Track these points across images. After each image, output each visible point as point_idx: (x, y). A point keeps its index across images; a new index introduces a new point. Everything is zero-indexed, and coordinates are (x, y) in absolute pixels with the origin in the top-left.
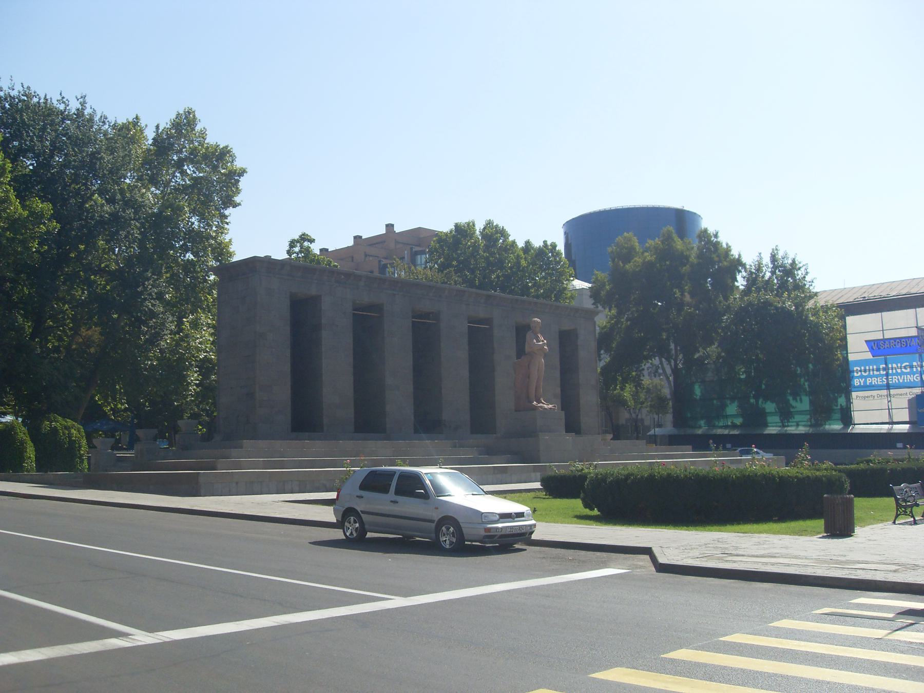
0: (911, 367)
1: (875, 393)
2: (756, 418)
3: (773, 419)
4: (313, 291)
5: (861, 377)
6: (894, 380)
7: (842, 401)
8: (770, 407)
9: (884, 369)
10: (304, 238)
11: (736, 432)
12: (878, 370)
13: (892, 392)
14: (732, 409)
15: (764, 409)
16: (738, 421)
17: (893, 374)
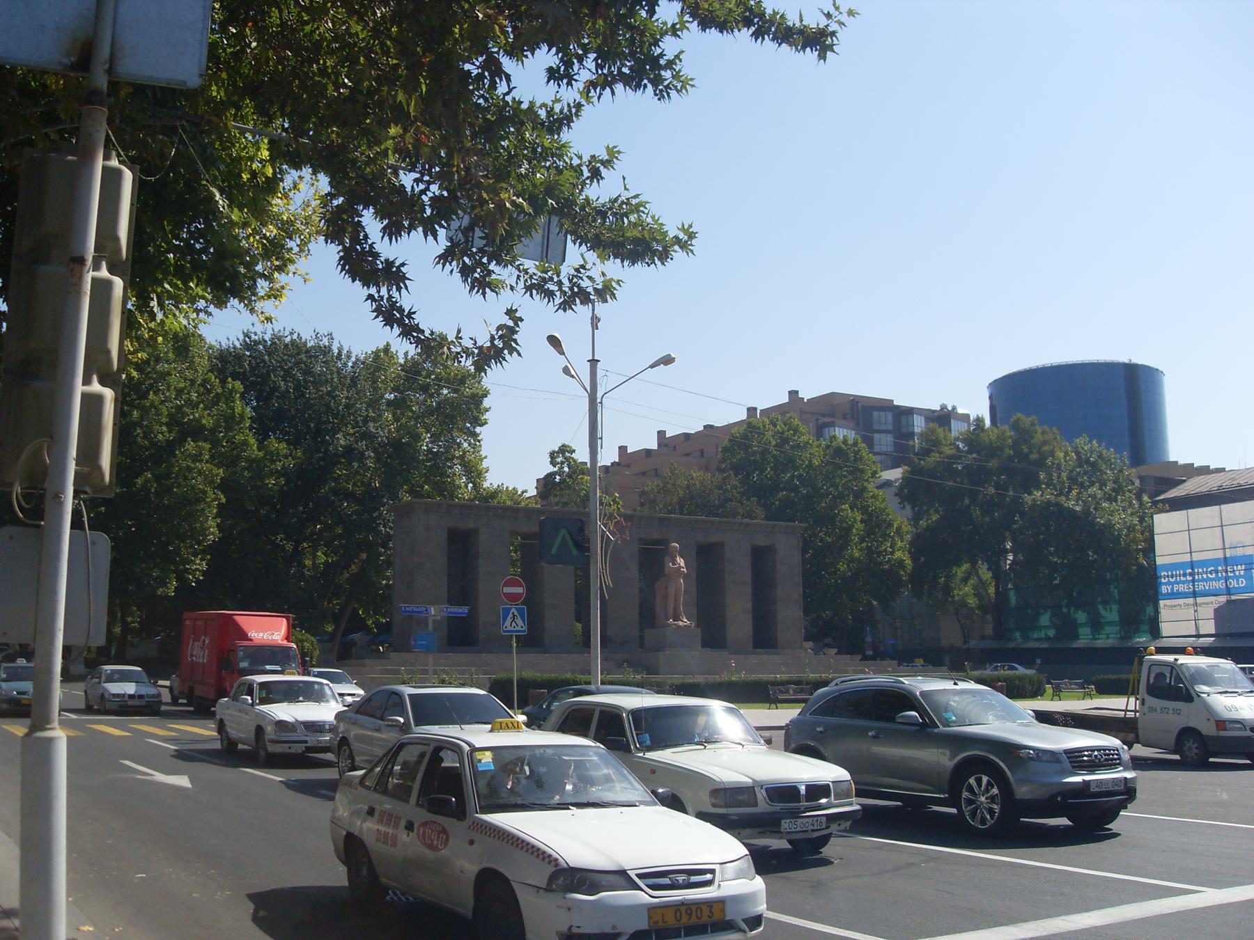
0: (1217, 572)
1: (1181, 601)
2: (1068, 629)
3: (1085, 632)
4: (471, 525)
5: (1169, 583)
6: (1200, 587)
7: (1150, 610)
8: (1081, 617)
9: (1190, 574)
10: (564, 449)
11: (1045, 645)
12: (1185, 575)
13: (1199, 600)
14: (1045, 619)
15: (1076, 620)
16: (1051, 633)
17: (1199, 581)
